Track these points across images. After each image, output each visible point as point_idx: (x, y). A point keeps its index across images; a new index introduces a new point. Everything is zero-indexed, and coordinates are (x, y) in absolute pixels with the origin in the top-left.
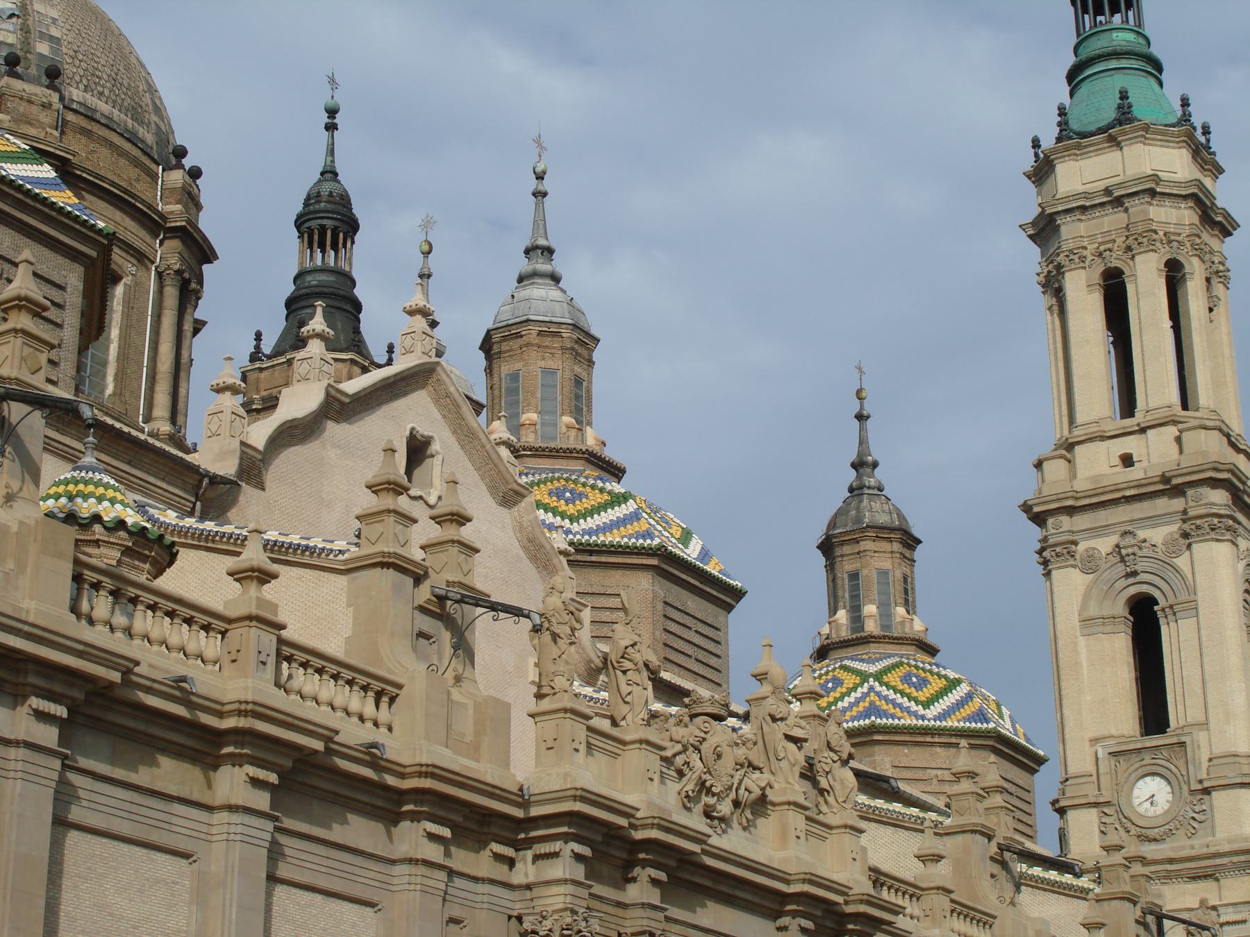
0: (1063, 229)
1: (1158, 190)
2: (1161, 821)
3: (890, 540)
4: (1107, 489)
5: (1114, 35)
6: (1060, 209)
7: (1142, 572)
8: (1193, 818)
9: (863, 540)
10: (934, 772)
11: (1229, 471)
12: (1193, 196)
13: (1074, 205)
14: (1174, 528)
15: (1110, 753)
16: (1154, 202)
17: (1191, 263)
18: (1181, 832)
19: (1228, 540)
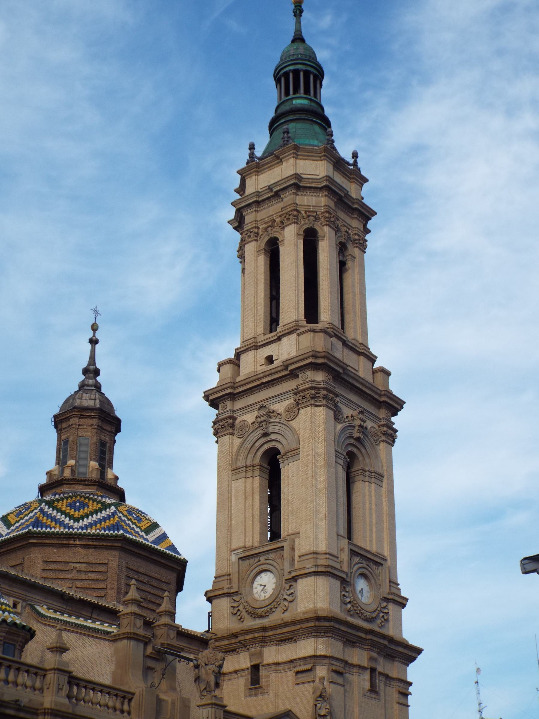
0: (246, 218)
1: (301, 185)
2: (267, 603)
3: (90, 417)
4: (252, 379)
5: (294, 102)
6: (243, 205)
7: (272, 433)
8: (285, 599)
9: (72, 418)
10: (75, 565)
11: (324, 357)
12: (326, 187)
13: (251, 201)
14: (291, 401)
15: (240, 558)
16: (300, 194)
17: (323, 230)
18: (279, 610)
19: (323, 405)
